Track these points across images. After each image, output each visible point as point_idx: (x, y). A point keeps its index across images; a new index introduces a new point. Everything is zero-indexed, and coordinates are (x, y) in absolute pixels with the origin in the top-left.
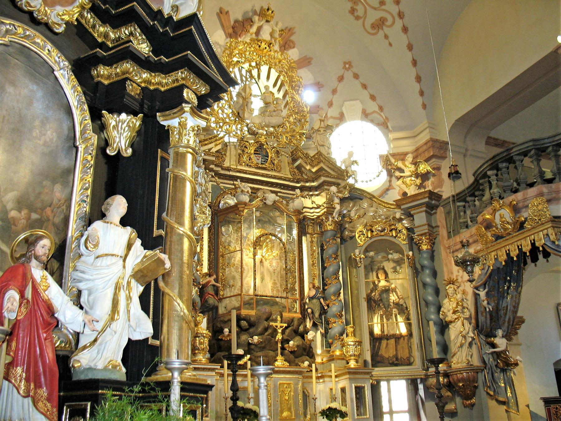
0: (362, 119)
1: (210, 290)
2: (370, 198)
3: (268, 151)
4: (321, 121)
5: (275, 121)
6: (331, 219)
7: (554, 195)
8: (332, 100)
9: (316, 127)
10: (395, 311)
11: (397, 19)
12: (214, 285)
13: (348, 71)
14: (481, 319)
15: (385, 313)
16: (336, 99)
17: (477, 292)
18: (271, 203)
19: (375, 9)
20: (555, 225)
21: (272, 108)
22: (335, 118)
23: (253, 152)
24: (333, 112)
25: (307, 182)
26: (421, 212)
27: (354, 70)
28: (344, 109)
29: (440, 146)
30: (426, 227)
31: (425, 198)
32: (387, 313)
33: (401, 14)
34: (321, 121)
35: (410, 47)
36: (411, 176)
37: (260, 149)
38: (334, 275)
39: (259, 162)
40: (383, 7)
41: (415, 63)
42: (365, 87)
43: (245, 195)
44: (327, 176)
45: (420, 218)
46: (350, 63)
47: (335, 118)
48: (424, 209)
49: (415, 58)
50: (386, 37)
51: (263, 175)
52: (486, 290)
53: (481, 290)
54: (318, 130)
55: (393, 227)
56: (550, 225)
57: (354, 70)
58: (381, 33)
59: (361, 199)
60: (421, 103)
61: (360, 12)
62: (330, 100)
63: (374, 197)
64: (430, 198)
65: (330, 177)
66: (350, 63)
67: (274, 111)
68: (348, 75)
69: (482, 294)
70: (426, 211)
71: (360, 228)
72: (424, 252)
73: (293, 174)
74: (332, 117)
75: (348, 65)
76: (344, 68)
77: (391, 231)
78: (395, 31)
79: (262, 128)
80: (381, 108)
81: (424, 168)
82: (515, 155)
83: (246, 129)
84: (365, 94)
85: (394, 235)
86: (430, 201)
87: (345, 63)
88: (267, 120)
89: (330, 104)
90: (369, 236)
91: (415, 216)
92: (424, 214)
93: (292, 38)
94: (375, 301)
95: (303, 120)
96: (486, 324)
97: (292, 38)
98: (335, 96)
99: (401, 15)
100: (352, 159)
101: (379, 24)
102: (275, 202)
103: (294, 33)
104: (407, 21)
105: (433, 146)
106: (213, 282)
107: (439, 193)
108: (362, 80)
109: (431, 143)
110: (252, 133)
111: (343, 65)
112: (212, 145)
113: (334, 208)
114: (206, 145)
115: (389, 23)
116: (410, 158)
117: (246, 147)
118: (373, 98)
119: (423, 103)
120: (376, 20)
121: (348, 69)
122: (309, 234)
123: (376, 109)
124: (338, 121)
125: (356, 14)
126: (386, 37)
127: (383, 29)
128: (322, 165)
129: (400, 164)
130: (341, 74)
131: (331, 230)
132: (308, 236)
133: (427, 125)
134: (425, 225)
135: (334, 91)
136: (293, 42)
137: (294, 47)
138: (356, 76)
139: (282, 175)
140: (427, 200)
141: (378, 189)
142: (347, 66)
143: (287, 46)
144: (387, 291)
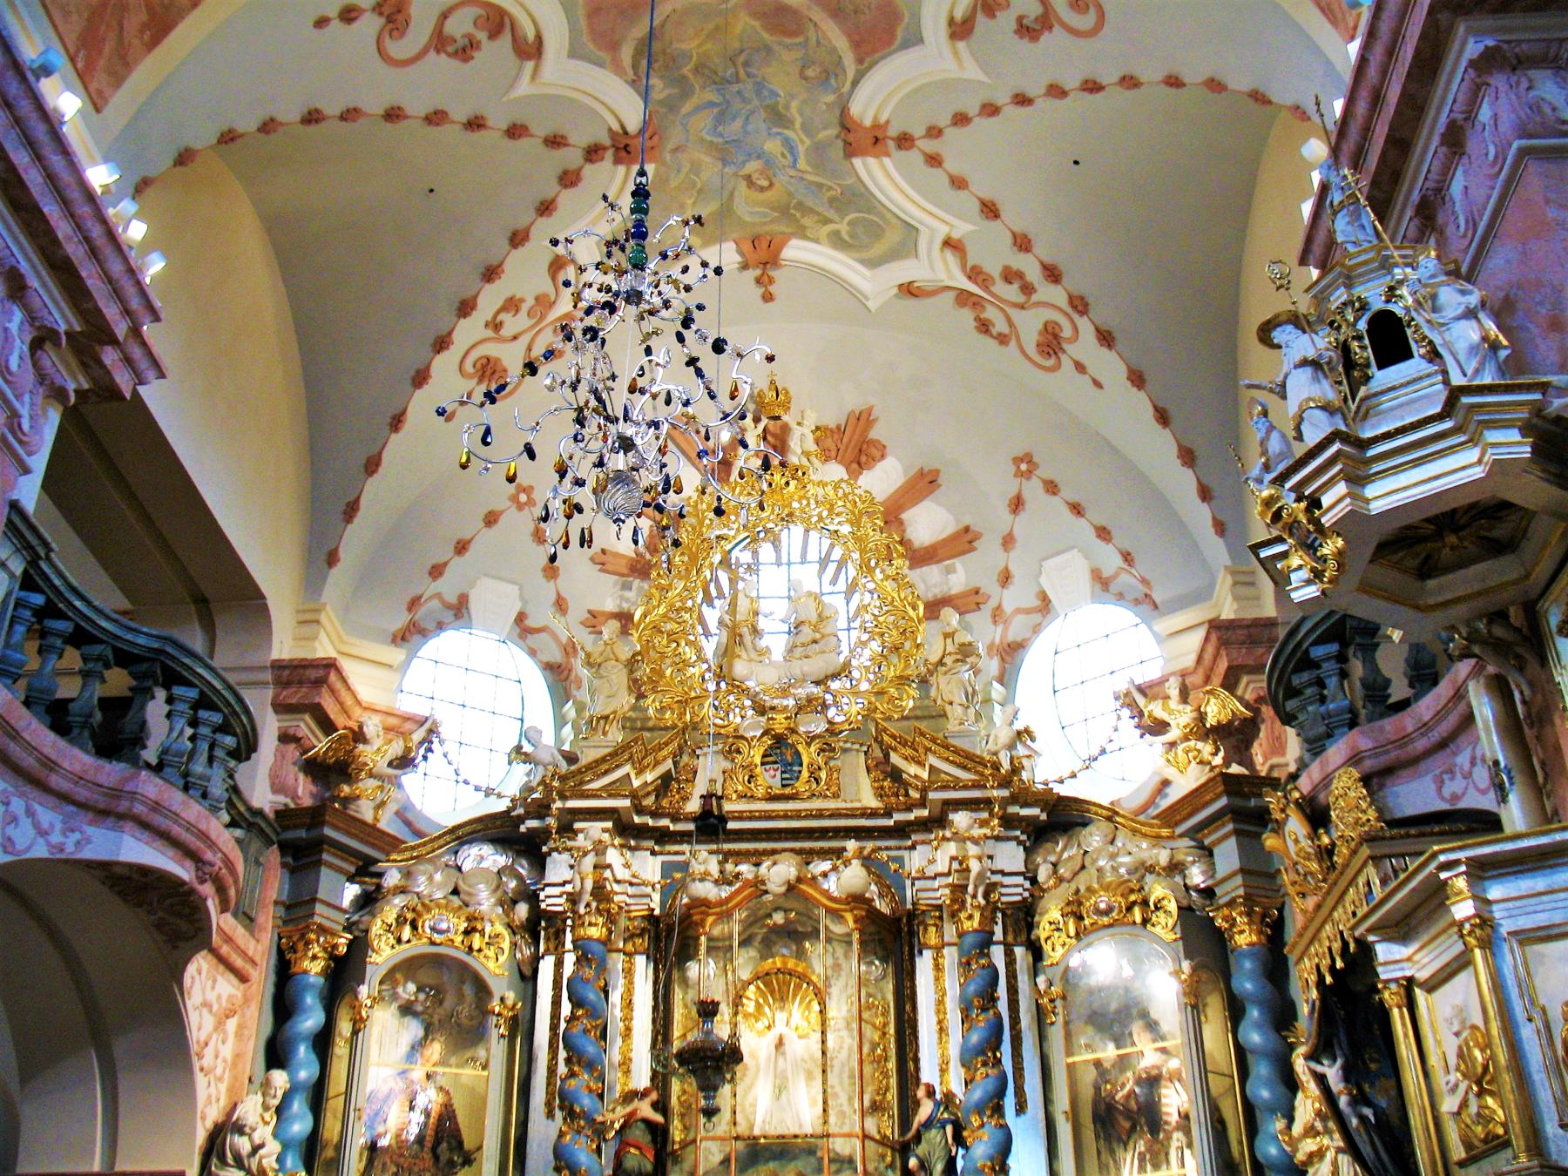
0: (1095, 599)
1: (639, 1134)
2: (1109, 819)
3: (800, 748)
4: (946, 636)
5: (817, 665)
6: (969, 900)
7: (1393, 755)
8: (1007, 569)
9: (934, 658)
10: (1178, 1138)
11: (1075, 316)
12: (646, 1121)
13: (1029, 479)
14: (1366, 1150)
15: (1149, 1149)
16: (1017, 561)
17: (1319, 1068)
18: (783, 889)
19: (1022, 307)
20: (1379, 852)
21: (807, 633)
22: (1028, 611)
23: (758, 760)
24: (1012, 599)
25: (909, 809)
26: (1226, 837)
27: (1044, 472)
28: (1044, 581)
29: (1250, 636)
30: (1239, 880)
31: (1218, 797)
32: (1157, 1147)
33: (1077, 302)
34: (946, 636)
35: (1137, 379)
36: (1186, 738)
37: (780, 748)
38: (977, 1055)
39: (777, 782)
40: (1035, 298)
41: (1163, 417)
42: (1077, 509)
43: (702, 880)
44: (945, 788)
45: (1228, 856)
46: (1028, 458)
47: (1028, 611)
48: (1230, 827)
49: (1160, 404)
50: (1080, 367)
51: (786, 816)
52: (1339, 1062)
53: (1325, 1062)
54: (941, 663)
55: (1133, 898)
56: (1365, 851)
57: (1044, 472)
58: (1066, 362)
59: (1085, 825)
60: (1210, 522)
61: (1000, 326)
62: (1002, 565)
63: (1117, 813)
64: (1228, 793)
65: (954, 788)
66: (1028, 458)
67: (815, 642)
68: (1033, 491)
69: (1333, 1072)
70: (1237, 832)
71: (1054, 914)
72: (1243, 955)
73: (880, 793)
74: (1018, 611)
75: (1025, 464)
76: (1019, 474)
77: (1129, 909)
78: (1085, 346)
79: (784, 692)
80: (1127, 557)
81: (1217, 710)
82: (1315, 643)
83: (748, 703)
84: (1083, 529)
85: (1138, 919)
86: (1239, 802)
87: (1017, 461)
88: (798, 667)
89: (1005, 578)
90: (1072, 933)
91: (1216, 851)
92: (1232, 842)
93: (873, 434)
94: (1128, 1114)
95: (908, 645)
96: (1383, 1164)
97: (873, 434)
98: (1013, 554)
99: (1079, 305)
100: (1019, 726)
101: (1051, 343)
102: (791, 888)
103: (875, 420)
104: (1103, 312)
105: (1224, 643)
106: (645, 1109)
107: (1275, 774)
108: (1068, 493)
109: (1214, 638)
110: (761, 710)
111: (1013, 469)
112: (627, 769)
113: (968, 870)
114: (606, 772)
115: (1067, 332)
116: (1173, 689)
117: (738, 752)
118: (1103, 533)
119: (1214, 519)
120: (1040, 333)
121: (1028, 474)
122: (930, 947)
123: (1118, 561)
124: (1037, 617)
125: (994, 331)
126: (1080, 367)
127: (1064, 351)
128: (932, 760)
129: (1156, 709)
130: (1013, 492)
131: (975, 931)
132: (927, 954)
133: (1229, 580)
134: (1233, 874)
135: (1008, 541)
136: (875, 443)
137: (883, 457)
138: (1051, 487)
139: (843, 805)
140: (1223, 801)
141: (1145, 783)
142: (1024, 467)
143: (863, 459)
144: (1152, 1081)
